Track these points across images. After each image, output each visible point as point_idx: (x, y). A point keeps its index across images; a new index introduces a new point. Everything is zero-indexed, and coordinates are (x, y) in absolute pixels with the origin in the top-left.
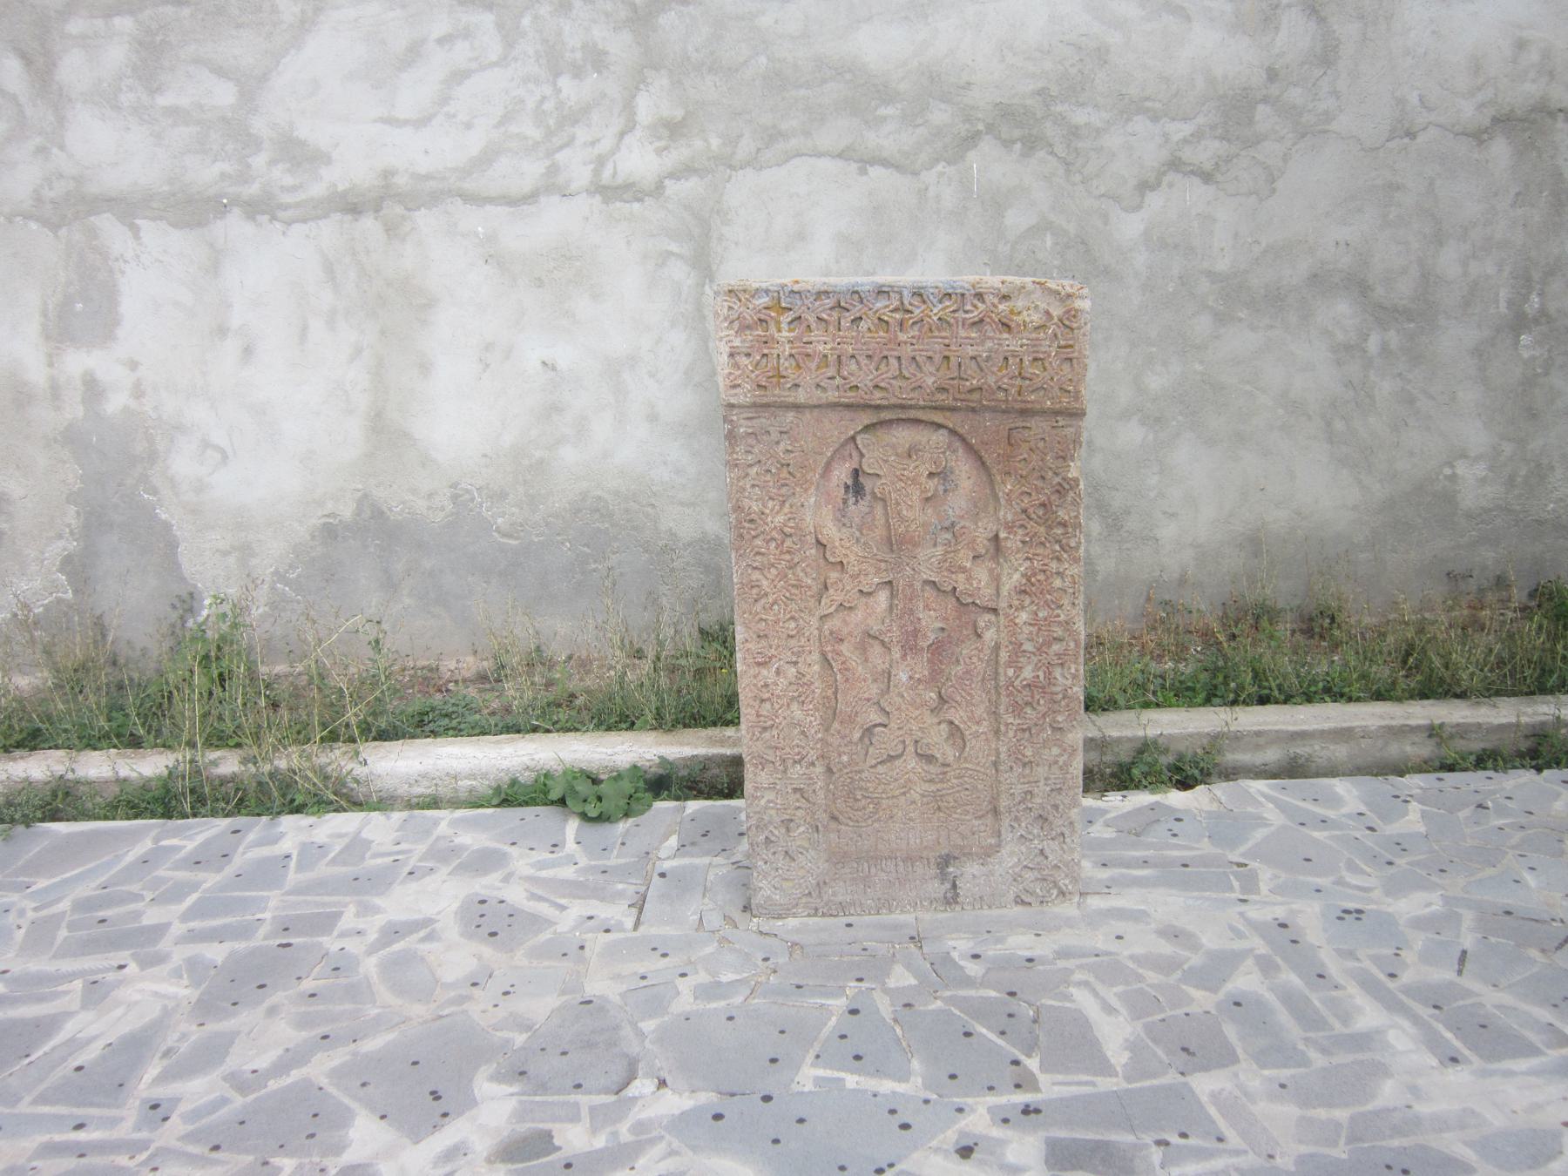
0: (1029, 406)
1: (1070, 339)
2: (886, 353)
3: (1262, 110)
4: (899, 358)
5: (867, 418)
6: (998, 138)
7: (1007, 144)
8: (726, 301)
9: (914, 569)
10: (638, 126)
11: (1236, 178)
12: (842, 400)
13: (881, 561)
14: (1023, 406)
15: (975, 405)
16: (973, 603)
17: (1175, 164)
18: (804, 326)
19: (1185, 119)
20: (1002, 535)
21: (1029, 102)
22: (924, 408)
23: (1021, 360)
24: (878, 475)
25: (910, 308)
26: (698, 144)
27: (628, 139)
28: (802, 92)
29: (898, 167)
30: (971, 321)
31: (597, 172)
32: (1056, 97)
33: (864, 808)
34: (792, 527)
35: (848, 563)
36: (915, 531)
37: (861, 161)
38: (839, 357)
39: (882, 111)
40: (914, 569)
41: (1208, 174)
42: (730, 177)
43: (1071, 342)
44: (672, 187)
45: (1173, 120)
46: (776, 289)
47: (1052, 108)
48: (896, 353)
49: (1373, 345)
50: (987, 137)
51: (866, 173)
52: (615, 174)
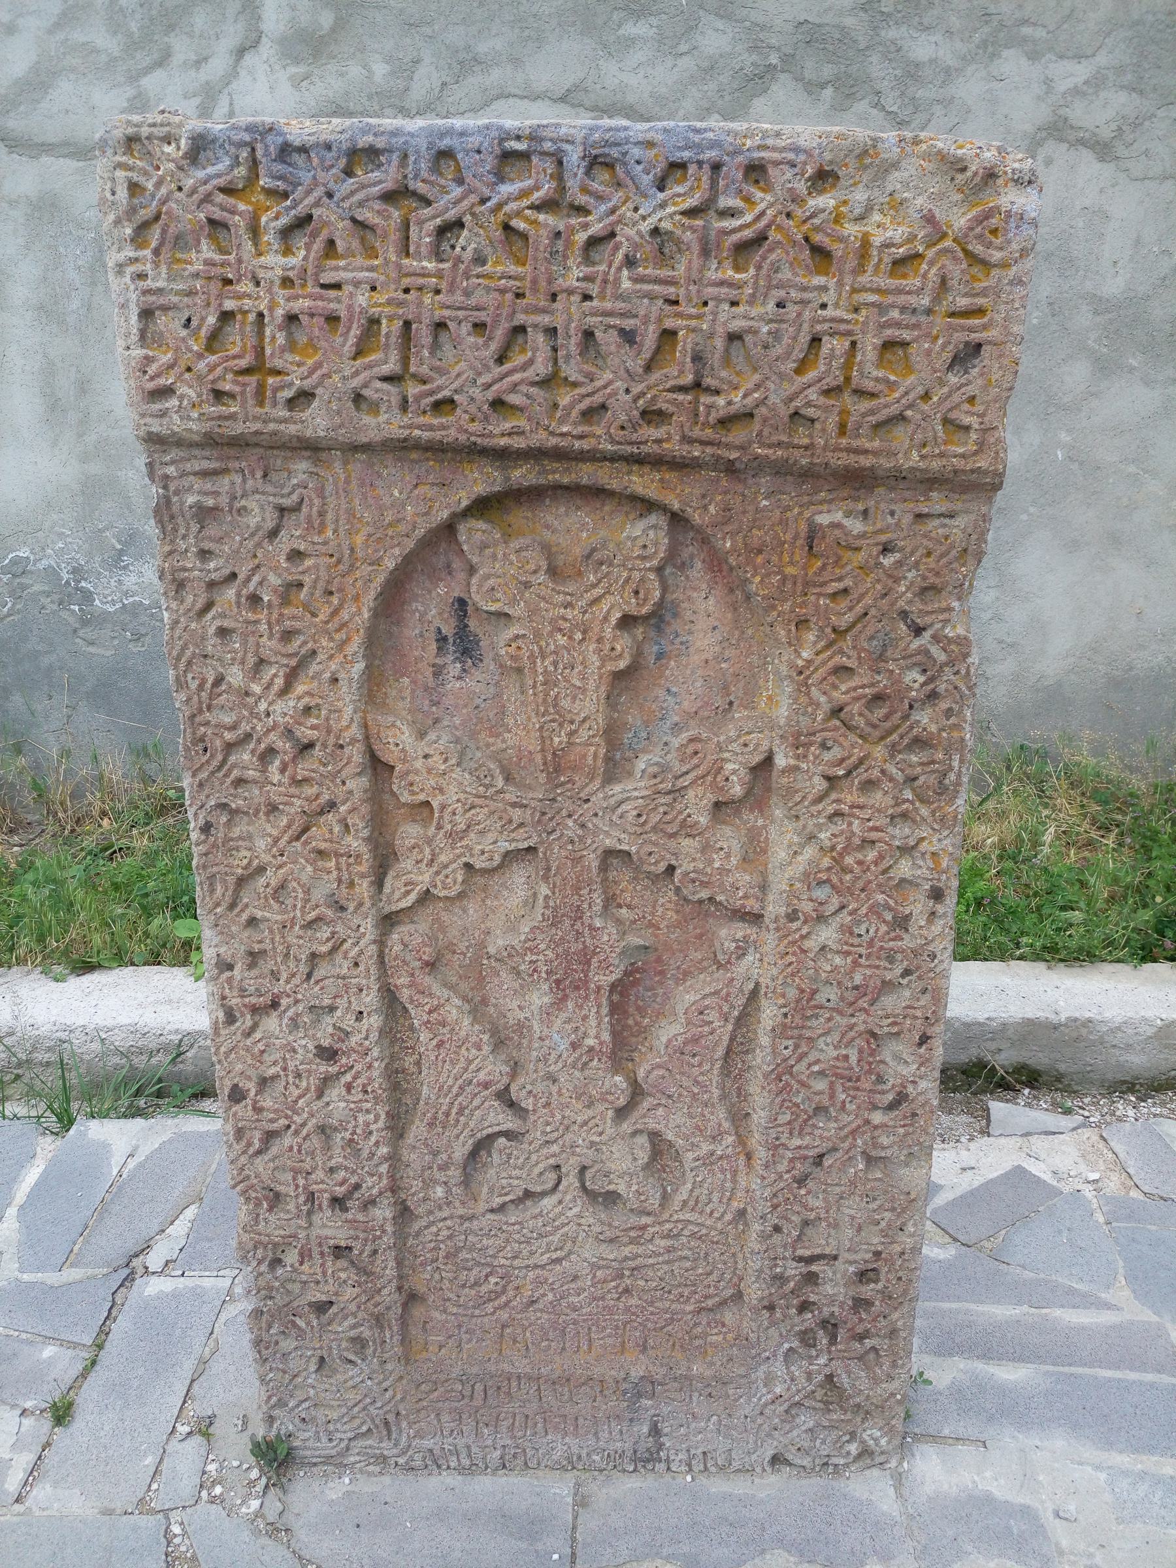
0: (866, 461)
1: (984, 293)
2: (521, 318)
4: (552, 332)
6: (799, 79)
7: (812, 88)
8: (120, 165)
9: (583, 826)
10: (264, 39)
11: (1146, 153)
13: (514, 805)
14: (850, 460)
15: (734, 455)
16: (711, 899)
18: (318, 245)
19: (1079, 57)
20: (781, 761)
21: (849, 21)
22: (613, 458)
23: (854, 344)
25: (582, 199)
26: (355, 71)
27: (249, 59)
30: (735, 238)
32: (889, 15)
34: (313, 727)
35: (443, 807)
36: (587, 744)
38: (407, 324)
39: (631, 29)
40: (583, 826)
41: (1106, 145)
43: (981, 301)
45: (1062, 57)
46: (247, 138)
47: (883, 33)
48: (546, 320)
50: (783, 76)
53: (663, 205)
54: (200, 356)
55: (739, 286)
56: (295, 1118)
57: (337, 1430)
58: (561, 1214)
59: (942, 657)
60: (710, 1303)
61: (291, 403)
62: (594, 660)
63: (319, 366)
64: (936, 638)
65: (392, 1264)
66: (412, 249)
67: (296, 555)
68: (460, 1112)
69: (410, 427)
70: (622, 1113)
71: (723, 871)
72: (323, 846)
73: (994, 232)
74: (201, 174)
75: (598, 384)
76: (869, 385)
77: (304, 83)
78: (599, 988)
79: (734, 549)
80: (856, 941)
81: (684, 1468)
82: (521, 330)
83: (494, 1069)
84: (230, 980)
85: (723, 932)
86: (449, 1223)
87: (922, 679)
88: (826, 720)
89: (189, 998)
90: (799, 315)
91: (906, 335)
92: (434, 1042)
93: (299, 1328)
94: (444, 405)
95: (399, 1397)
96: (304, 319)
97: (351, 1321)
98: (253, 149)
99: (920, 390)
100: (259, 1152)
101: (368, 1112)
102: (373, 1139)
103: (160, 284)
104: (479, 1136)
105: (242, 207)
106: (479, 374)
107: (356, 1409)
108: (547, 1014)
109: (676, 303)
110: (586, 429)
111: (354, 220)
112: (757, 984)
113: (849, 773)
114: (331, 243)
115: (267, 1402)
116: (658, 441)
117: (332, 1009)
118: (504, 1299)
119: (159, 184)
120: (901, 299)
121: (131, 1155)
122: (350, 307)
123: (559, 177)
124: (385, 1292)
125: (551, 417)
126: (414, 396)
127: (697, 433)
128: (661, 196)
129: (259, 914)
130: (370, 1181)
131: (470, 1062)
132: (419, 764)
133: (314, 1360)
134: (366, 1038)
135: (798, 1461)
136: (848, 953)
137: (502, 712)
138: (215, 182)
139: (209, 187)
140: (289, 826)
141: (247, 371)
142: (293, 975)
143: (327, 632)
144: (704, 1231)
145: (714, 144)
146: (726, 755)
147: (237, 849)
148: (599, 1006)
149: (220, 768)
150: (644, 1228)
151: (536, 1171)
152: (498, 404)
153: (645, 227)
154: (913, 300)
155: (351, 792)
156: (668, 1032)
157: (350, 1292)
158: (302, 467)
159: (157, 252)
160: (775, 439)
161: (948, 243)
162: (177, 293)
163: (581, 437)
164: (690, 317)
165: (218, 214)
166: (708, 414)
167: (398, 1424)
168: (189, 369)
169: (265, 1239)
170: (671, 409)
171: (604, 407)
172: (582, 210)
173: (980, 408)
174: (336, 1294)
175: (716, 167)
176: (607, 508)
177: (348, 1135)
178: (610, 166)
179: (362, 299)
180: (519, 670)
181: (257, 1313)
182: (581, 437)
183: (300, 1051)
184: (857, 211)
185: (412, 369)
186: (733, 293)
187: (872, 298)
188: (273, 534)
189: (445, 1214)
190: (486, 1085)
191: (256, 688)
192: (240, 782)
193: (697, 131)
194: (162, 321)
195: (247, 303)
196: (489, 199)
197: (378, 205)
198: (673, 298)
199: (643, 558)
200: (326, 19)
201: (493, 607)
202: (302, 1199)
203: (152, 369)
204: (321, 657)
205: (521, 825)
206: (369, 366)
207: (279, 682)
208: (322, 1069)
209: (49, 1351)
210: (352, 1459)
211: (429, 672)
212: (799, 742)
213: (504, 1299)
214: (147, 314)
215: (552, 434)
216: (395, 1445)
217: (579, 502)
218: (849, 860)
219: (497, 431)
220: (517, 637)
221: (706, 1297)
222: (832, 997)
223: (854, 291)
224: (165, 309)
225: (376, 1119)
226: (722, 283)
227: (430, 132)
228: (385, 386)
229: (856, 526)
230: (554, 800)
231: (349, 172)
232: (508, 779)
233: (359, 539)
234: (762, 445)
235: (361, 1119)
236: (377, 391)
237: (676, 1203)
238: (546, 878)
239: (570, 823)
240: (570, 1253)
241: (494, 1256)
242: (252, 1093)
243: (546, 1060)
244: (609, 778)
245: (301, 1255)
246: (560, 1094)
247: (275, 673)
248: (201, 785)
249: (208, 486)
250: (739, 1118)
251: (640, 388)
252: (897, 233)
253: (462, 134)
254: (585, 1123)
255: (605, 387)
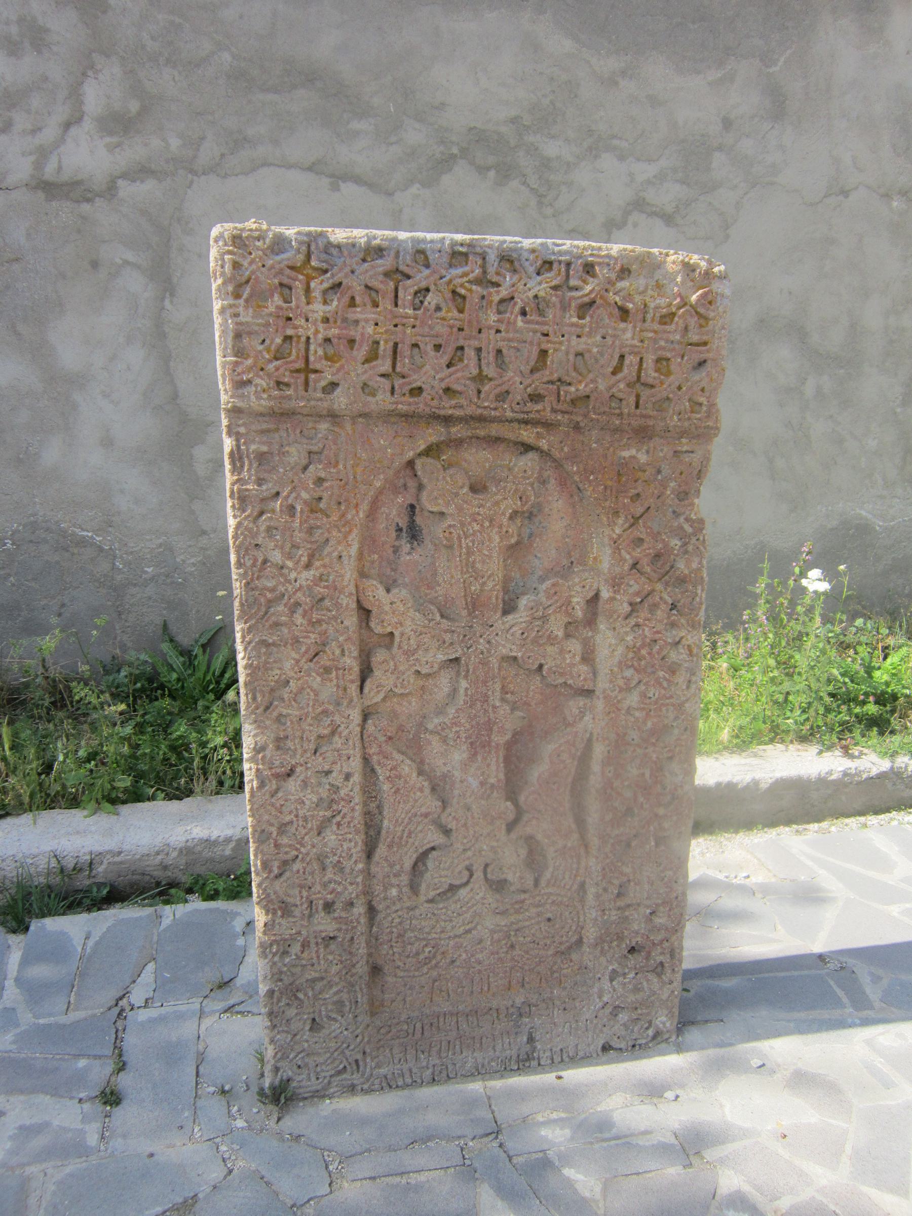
2: (461, 343)
3: (718, 159)
4: (479, 350)
5: (433, 434)
7: (482, 170)
8: (229, 252)
9: (489, 642)
10: (86, 118)
12: (400, 406)
13: (446, 631)
15: (579, 419)
16: (565, 683)
17: (639, 205)
18: (346, 299)
19: (649, 161)
20: (605, 594)
21: (503, 129)
23: (641, 359)
24: (442, 514)
25: (495, 279)
27: (73, 131)
28: (270, 97)
29: (371, 186)
30: (580, 301)
31: (39, 165)
33: (418, 954)
34: (325, 587)
35: (402, 634)
36: (491, 590)
37: (332, 176)
38: (396, 345)
39: (356, 125)
40: (489, 642)
42: (192, 182)
43: (705, 338)
44: (125, 189)
45: (638, 160)
47: (526, 138)
48: (476, 343)
49: (809, 389)
51: (339, 190)
52: (60, 168)
53: (540, 283)
54: (270, 361)
55: (583, 327)
56: (302, 850)
57: (323, 1071)
58: (472, 898)
59: (690, 530)
60: (563, 947)
61: (324, 390)
62: (497, 539)
63: (342, 367)
64: (687, 520)
65: (363, 945)
66: (400, 303)
67: (320, 481)
68: (409, 836)
69: (397, 403)
70: (510, 827)
71: (572, 665)
72: (328, 663)
73: (710, 303)
74: (278, 258)
75: (505, 379)
76: (650, 381)
77: (117, 150)
78: (498, 745)
79: (578, 472)
80: (648, 701)
81: (549, 1061)
82: (462, 348)
83: (431, 804)
84: (263, 757)
85: (571, 703)
86: (400, 913)
87: (679, 543)
88: (631, 570)
89: (93, 828)
90: (613, 342)
91: (669, 355)
92: (393, 790)
93: (300, 1000)
94: (417, 391)
95: (366, 1039)
96: (335, 341)
97: (335, 989)
98: (309, 246)
99: (677, 384)
100: (277, 877)
101: (350, 841)
102: (353, 859)
103: (249, 319)
104: (421, 851)
105: (301, 277)
106: (437, 373)
107: (336, 1054)
108: (465, 766)
109: (547, 335)
110: (499, 404)
111: (367, 286)
112: (591, 734)
113: (642, 601)
114: (353, 298)
115: (275, 1057)
116: (538, 411)
117: (328, 773)
118: (434, 962)
119: (251, 263)
120: (665, 336)
121: (87, 938)
122: (362, 334)
123: (484, 267)
124: (358, 966)
125: (479, 398)
126: (399, 385)
127: (559, 407)
128: (539, 278)
129: (285, 712)
130: (350, 888)
131: (416, 801)
132: (387, 608)
133: (309, 1022)
134: (351, 791)
135: (618, 1046)
136: (643, 709)
137: (435, 574)
138: (286, 263)
139: (282, 265)
140: (306, 652)
141: (298, 371)
142: (305, 751)
143: (336, 526)
144: (560, 899)
145: (566, 253)
146: (573, 593)
147: (272, 669)
148: (498, 758)
149: (263, 616)
150: (523, 902)
151: (457, 870)
152: (447, 390)
153: (531, 294)
154: (671, 338)
155: (347, 628)
156: (537, 772)
157: (334, 969)
158: (324, 426)
159: (247, 301)
160: (602, 410)
161: (687, 307)
162: (258, 325)
163: (495, 409)
164: (555, 343)
165: (286, 281)
166: (566, 396)
167: (364, 1060)
168: (262, 369)
169: (278, 938)
170: (546, 393)
171: (507, 392)
172: (498, 285)
173: (707, 394)
174: (326, 971)
175: (568, 264)
176: (500, 449)
177: (336, 858)
178: (511, 262)
179: (370, 330)
180: (450, 547)
181: (271, 993)
182: (495, 409)
183: (307, 802)
184: (641, 289)
185: (398, 369)
186: (578, 330)
187: (651, 335)
188: (305, 468)
189: (398, 907)
190: (426, 815)
191: (290, 564)
192: (277, 624)
193: (558, 245)
194: (246, 341)
195: (301, 331)
196: (445, 277)
197: (381, 278)
198: (546, 332)
199: (524, 478)
200: (134, 106)
201: (435, 509)
202: (305, 906)
203: (239, 369)
204: (332, 543)
205: (452, 644)
206: (374, 367)
207: (305, 559)
208: (321, 813)
209: (82, 1063)
210: (332, 1090)
211: (390, 551)
212: (616, 583)
213: (434, 962)
214: (238, 336)
215: (478, 407)
216: (363, 1075)
217: (485, 446)
218: (644, 652)
219: (447, 405)
220: (450, 526)
221: (561, 943)
222: (635, 737)
223: (641, 331)
224: (250, 333)
225: (357, 846)
226: (573, 325)
227: (413, 239)
228: (382, 380)
229: (643, 458)
230: (471, 627)
231: (364, 260)
232: (442, 616)
233: (359, 470)
234: (595, 413)
235: (346, 845)
236: (377, 382)
237: (543, 883)
238: (466, 677)
239: (482, 641)
240: (478, 924)
241: (429, 933)
242: (275, 834)
243: (464, 795)
244: (505, 612)
245: (303, 946)
246: (473, 818)
247: (302, 554)
248: (249, 628)
249: (265, 439)
250: (580, 822)
251: (529, 381)
252: (662, 302)
253: (432, 241)
254: (489, 834)
255: (509, 381)
